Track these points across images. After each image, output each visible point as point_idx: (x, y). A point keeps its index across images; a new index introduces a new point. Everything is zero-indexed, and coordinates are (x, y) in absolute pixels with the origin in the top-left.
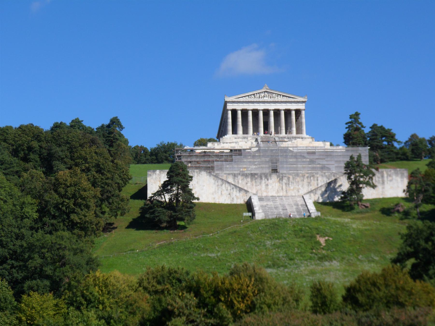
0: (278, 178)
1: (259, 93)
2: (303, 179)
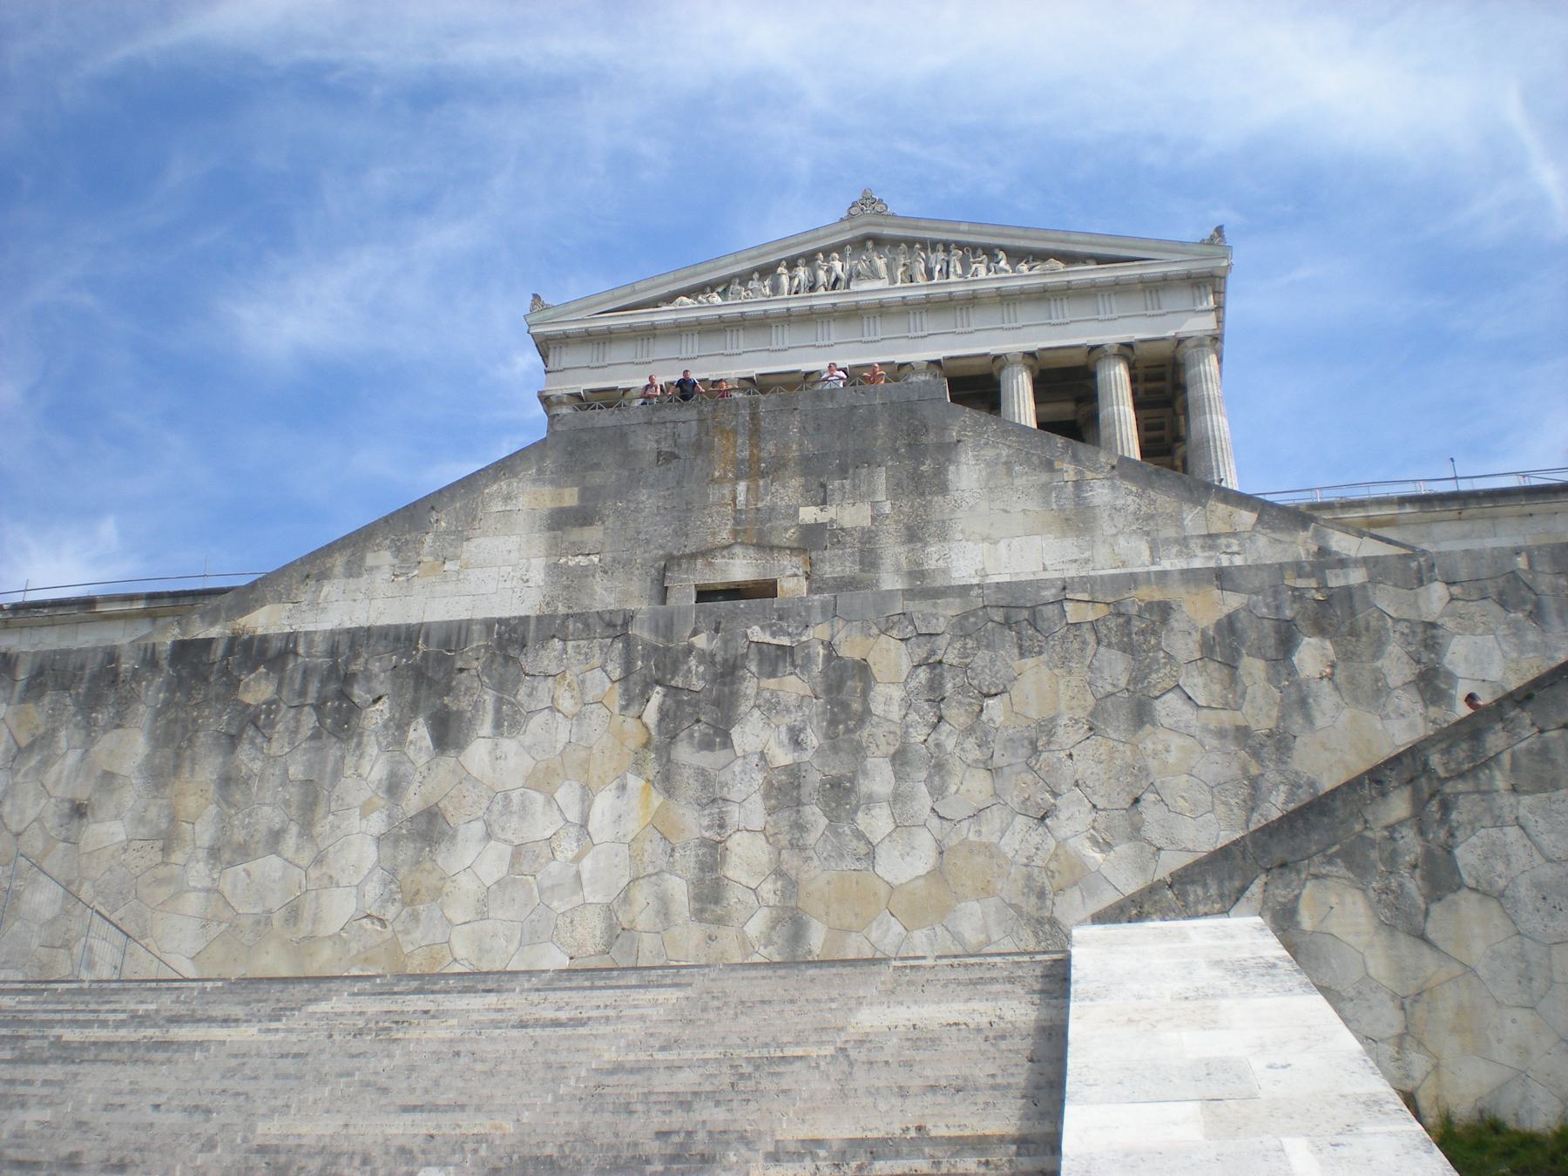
0: (634, 697)
1: (810, 258)
2: (1139, 677)
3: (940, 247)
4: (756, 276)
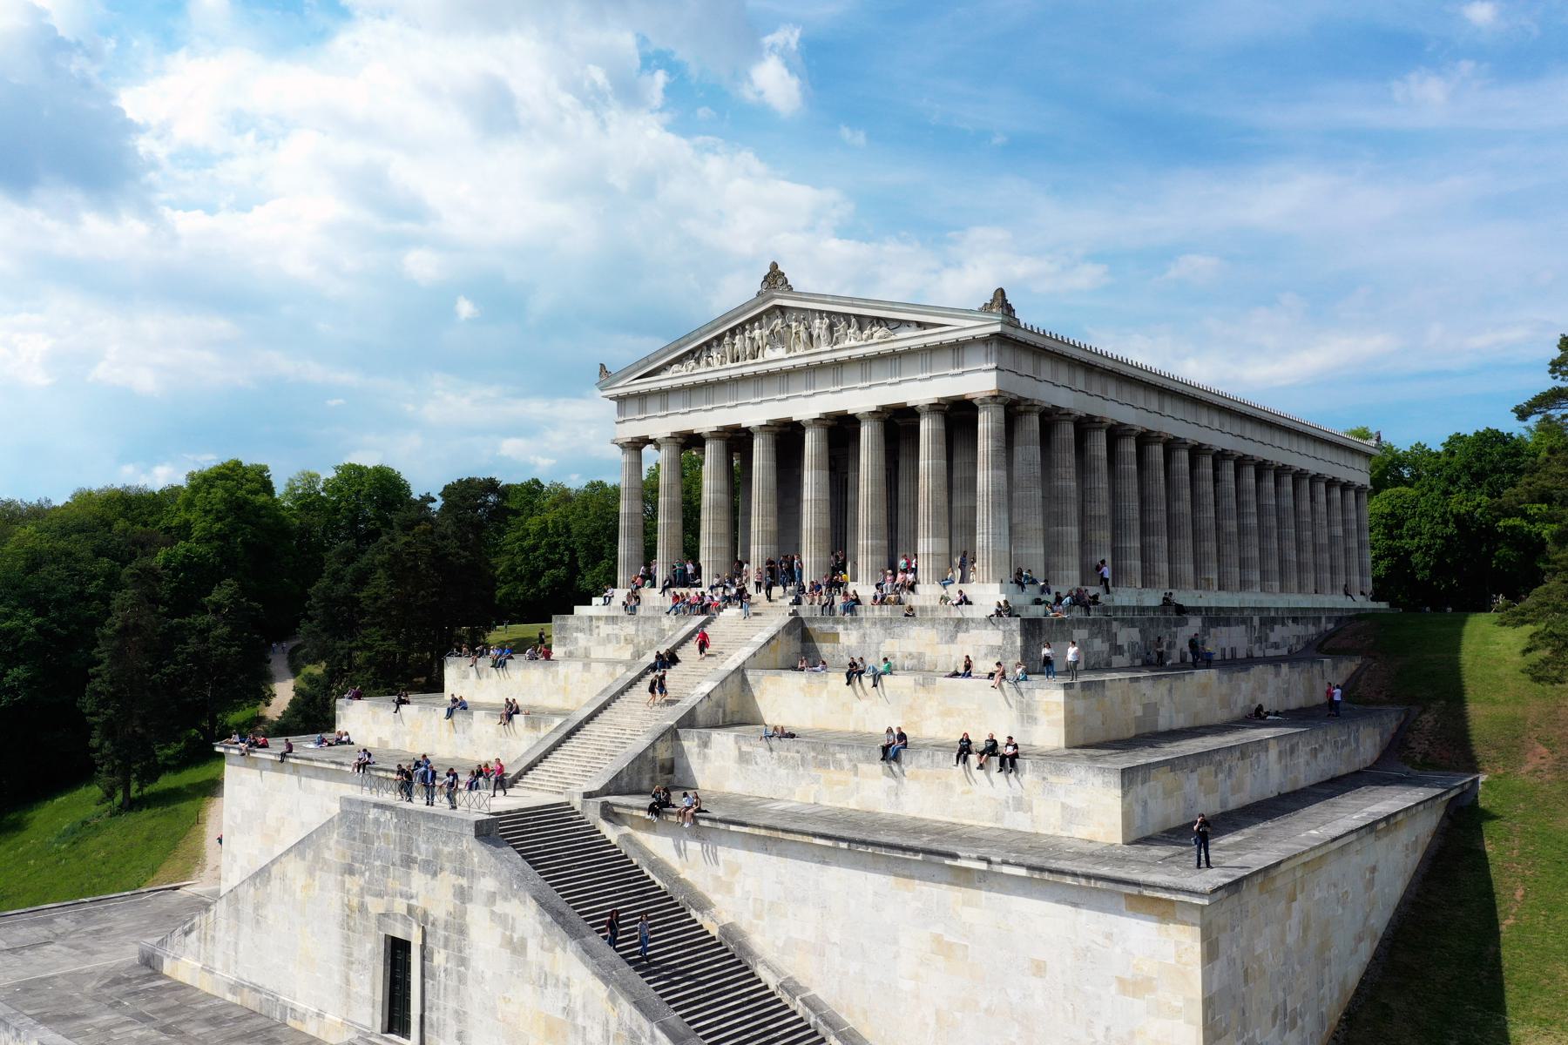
4: (715, 344)
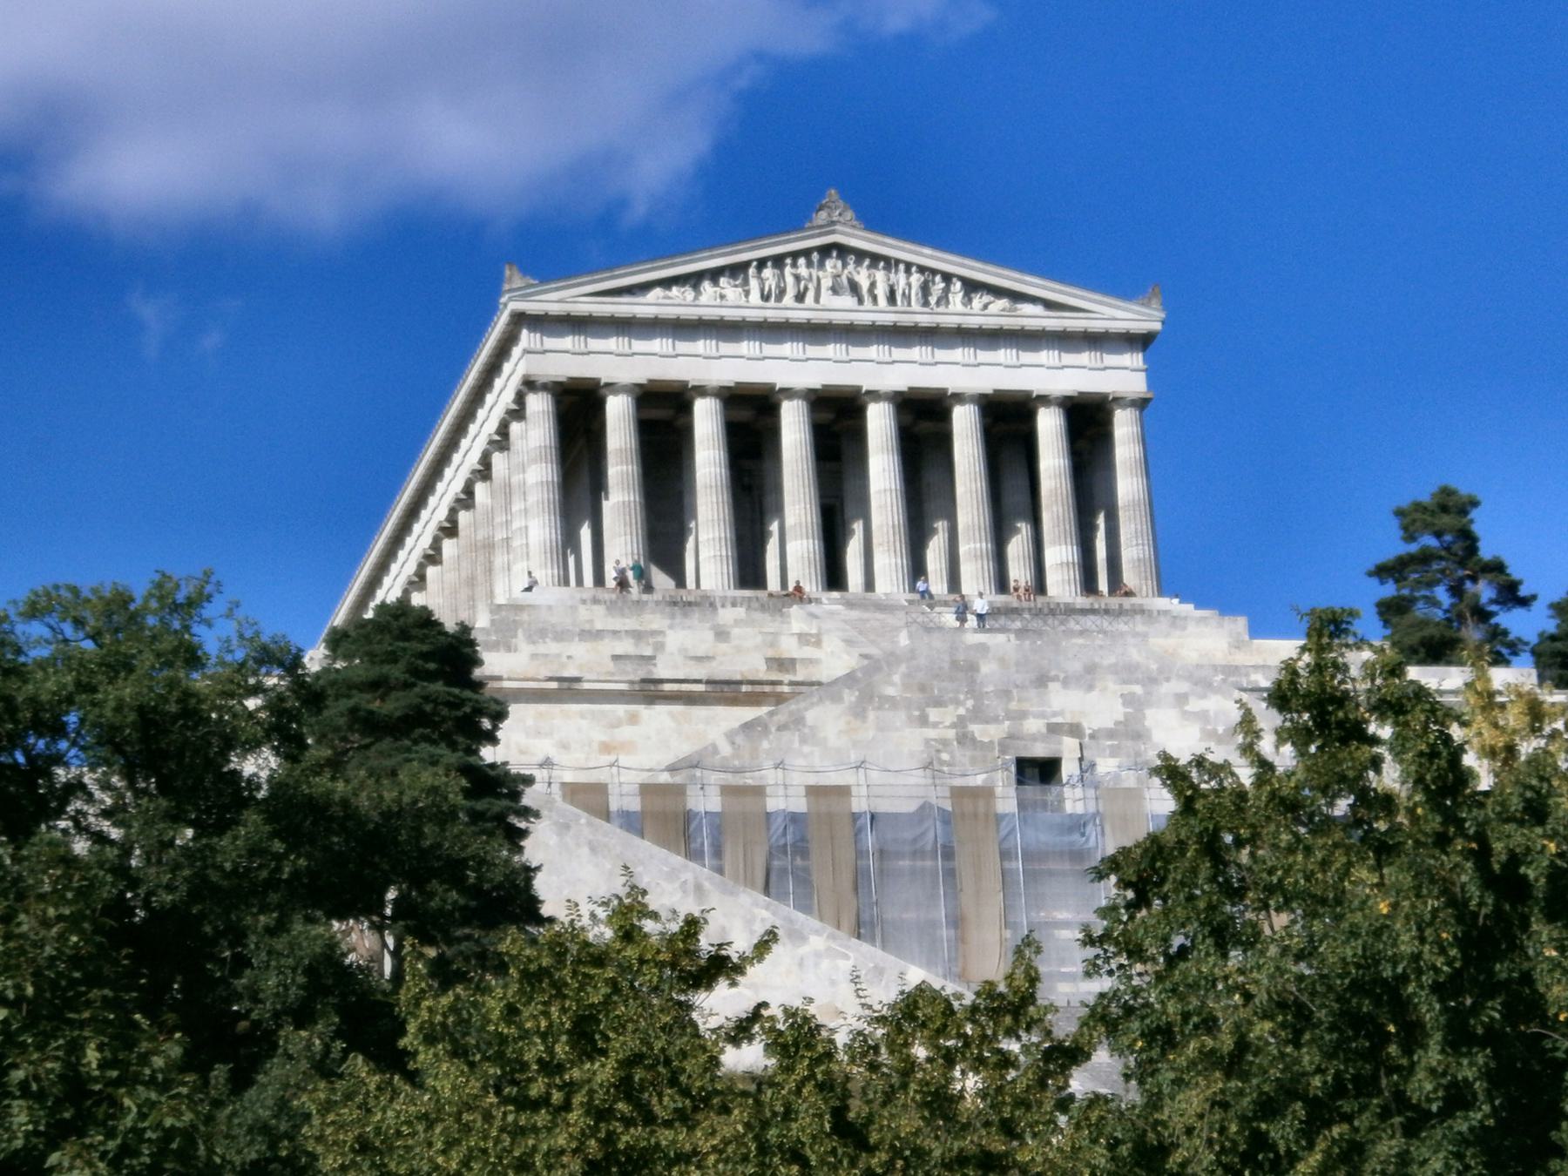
1: (778, 261)
3: (902, 267)
